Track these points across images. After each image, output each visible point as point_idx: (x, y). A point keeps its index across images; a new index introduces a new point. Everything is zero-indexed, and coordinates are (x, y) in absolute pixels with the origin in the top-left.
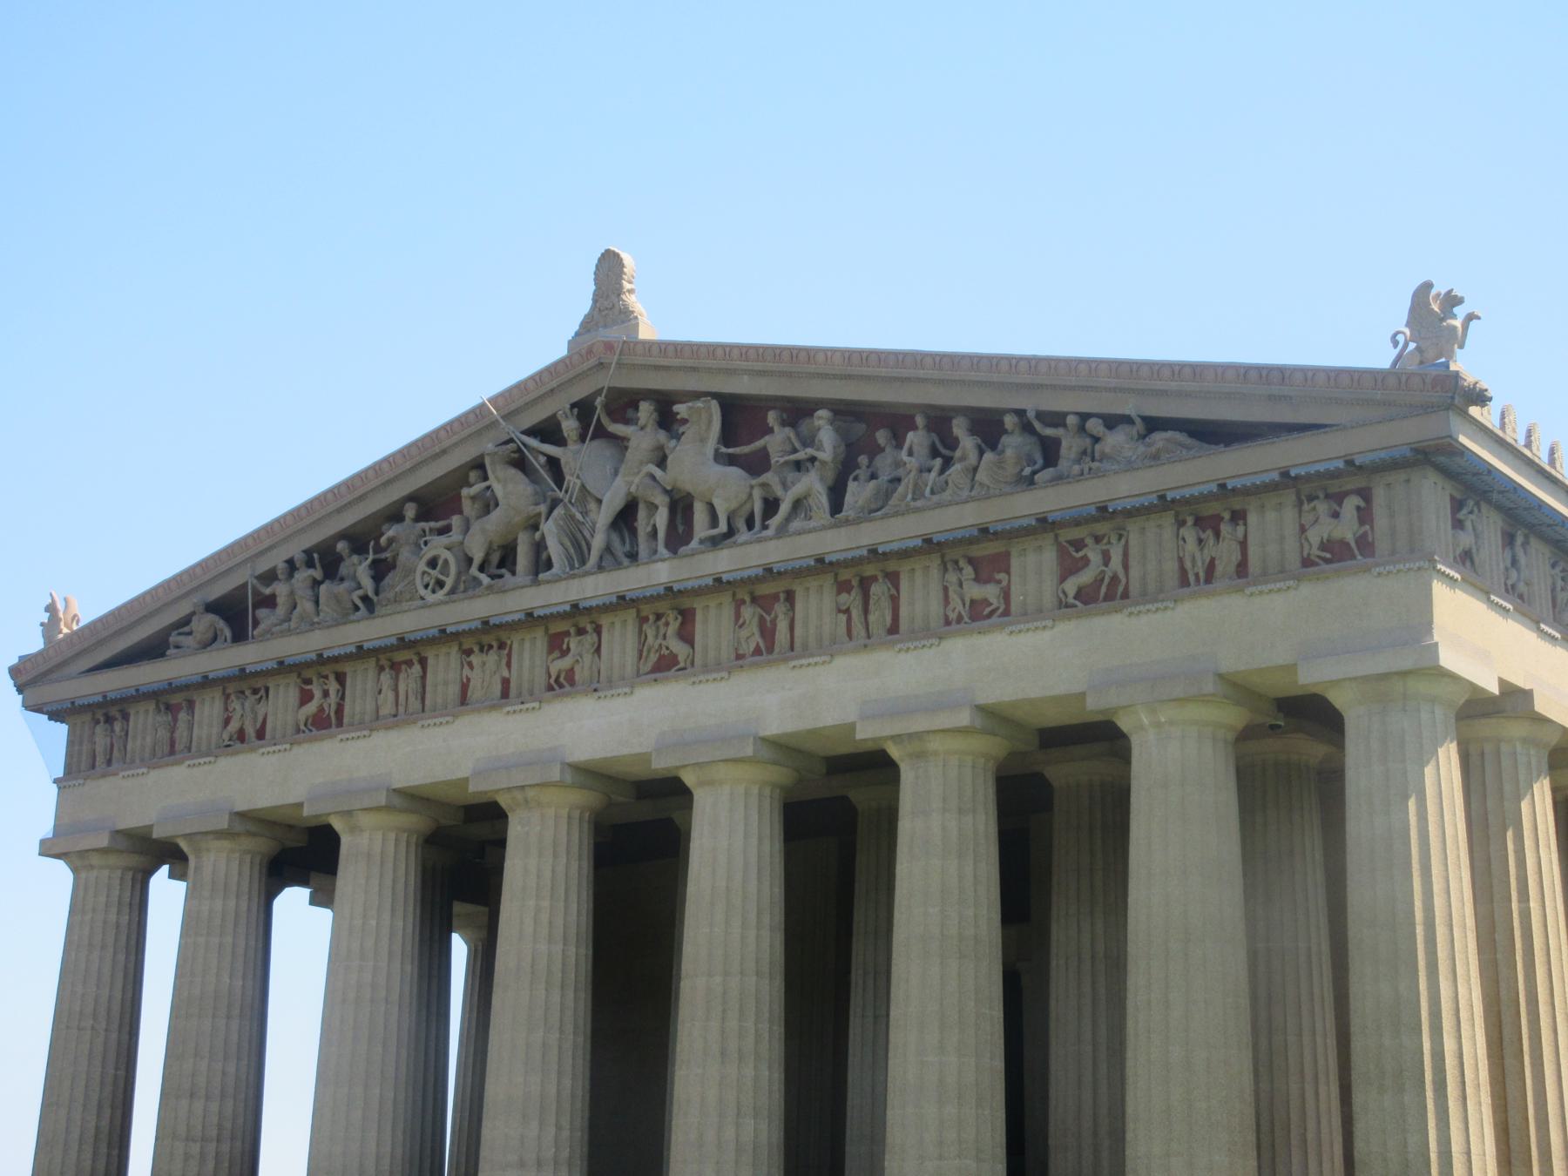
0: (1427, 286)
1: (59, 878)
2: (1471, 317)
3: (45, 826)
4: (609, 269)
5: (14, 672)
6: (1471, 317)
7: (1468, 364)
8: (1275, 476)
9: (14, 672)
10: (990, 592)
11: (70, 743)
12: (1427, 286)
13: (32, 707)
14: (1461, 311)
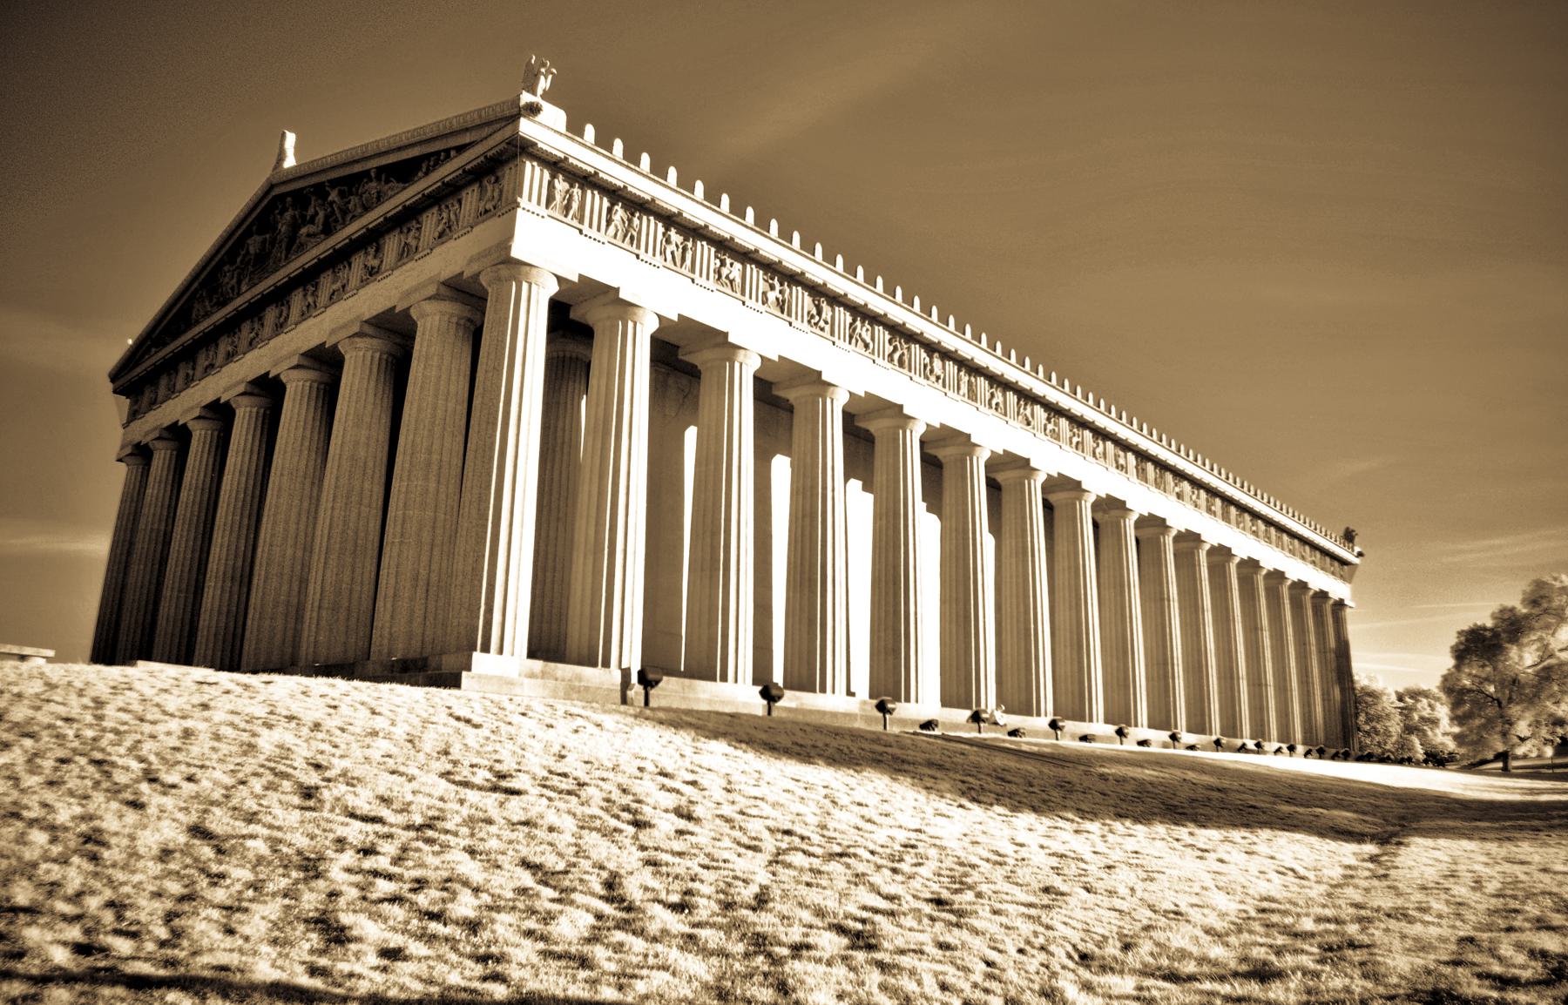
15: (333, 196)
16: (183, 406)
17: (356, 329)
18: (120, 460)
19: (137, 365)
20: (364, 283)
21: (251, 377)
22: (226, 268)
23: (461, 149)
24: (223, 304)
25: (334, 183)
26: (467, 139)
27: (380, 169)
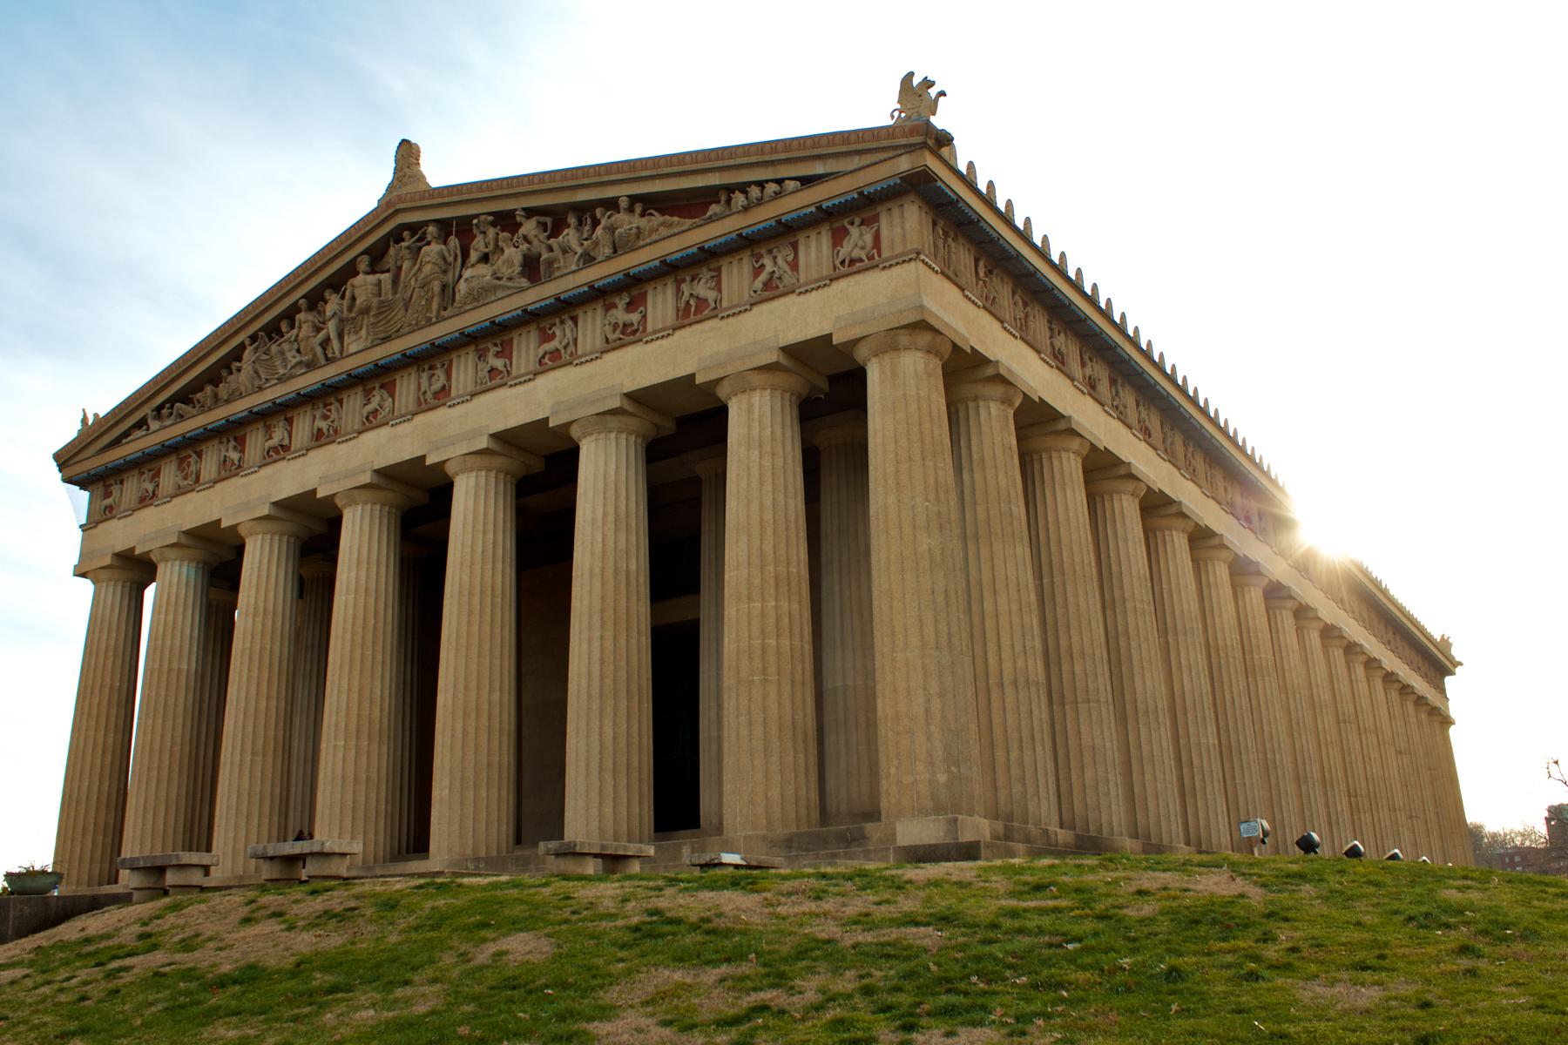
0: (911, 74)
1: (85, 589)
2: (942, 94)
3: (73, 557)
4: (407, 153)
5: (57, 457)
6: (942, 94)
7: (939, 121)
8: (813, 209)
9: (57, 457)
10: (634, 317)
11: (90, 503)
12: (911, 74)
13: (68, 480)
14: (933, 92)
15: (529, 227)
16: (243, 496)
17: (615, 403)
18: (84, 575)
19: (117, 442)
20: (611, 346)
21: (381, 463)
22: (301, 317)
23: (807, 181)
24: (311, 366)
25: (530, 212)
26: (818, 168)
27: (634, 199)
